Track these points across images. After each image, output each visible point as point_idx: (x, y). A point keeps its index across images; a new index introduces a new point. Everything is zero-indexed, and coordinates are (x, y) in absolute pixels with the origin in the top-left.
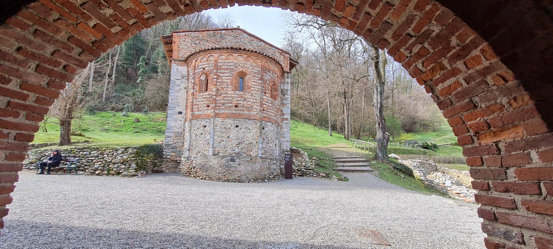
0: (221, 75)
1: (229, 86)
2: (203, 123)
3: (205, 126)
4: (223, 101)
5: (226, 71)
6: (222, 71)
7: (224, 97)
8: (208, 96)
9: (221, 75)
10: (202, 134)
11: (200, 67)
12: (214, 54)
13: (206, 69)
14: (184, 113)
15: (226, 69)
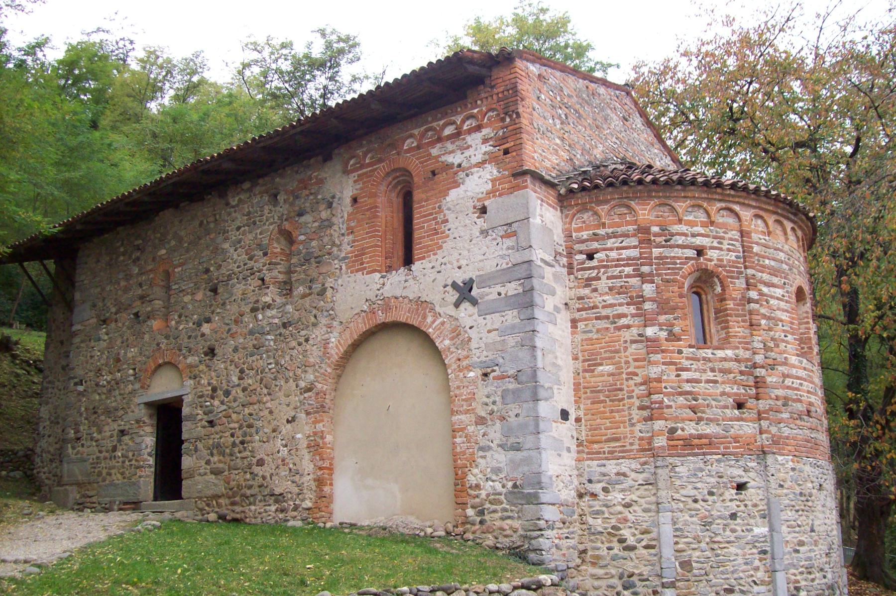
0: (765, 290)
1: (790, 338)
2: (737, 473)
3: (741, 487)
4: (780, 392)
5: (775, 280)
6: (765, 277)
7: (785, 376)
8: (732, 365)
9: (765, 290)
10: (733, 516)
11: (680, 240)
12: (737, 208)
13: (712, 254)
14: (572, 417)
15: (774, 272)
